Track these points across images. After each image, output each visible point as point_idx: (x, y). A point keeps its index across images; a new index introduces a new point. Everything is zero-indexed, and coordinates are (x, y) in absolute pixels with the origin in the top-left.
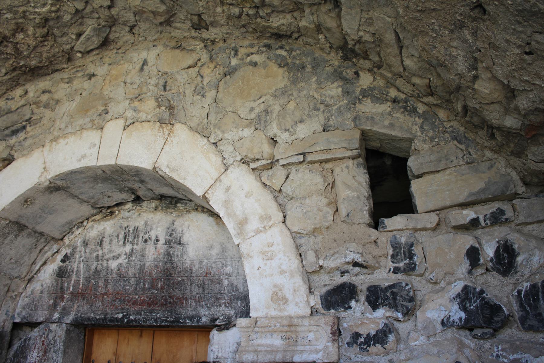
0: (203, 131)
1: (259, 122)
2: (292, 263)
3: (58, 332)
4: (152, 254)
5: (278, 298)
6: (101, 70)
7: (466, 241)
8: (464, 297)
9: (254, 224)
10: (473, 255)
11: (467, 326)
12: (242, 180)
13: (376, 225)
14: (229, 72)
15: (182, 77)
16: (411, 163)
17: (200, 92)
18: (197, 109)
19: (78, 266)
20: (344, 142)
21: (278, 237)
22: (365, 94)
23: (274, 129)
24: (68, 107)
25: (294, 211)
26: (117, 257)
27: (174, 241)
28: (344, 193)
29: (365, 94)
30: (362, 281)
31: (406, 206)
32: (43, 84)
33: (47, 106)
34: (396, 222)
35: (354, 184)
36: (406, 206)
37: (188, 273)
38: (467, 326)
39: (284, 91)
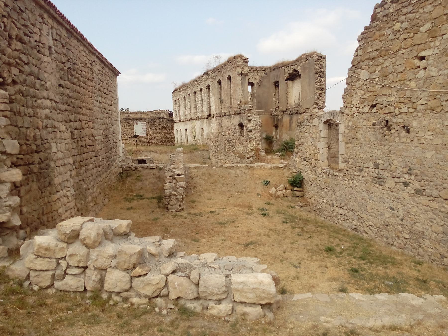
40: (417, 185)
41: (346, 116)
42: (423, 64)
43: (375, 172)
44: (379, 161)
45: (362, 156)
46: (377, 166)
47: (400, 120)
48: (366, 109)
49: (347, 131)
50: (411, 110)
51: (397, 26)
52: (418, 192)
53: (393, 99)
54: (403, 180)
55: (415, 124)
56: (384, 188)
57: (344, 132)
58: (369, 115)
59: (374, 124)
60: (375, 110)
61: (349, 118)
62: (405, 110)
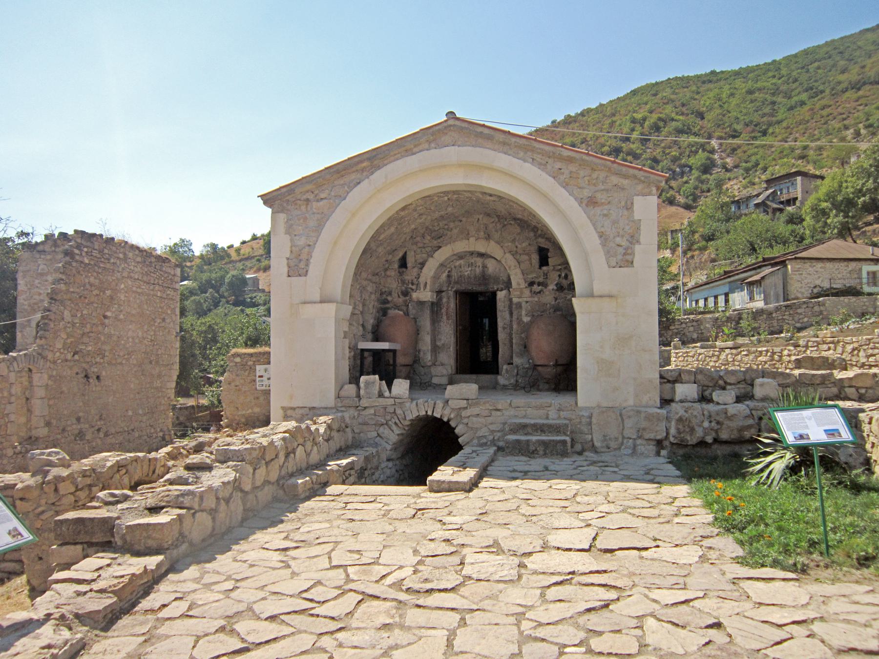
0: (498, 243)
1: (514, 241)
2: (521, 276)
3: (451, 293)
4: (478, 271)
5: (519, 284)
6: (464, 219)
7: (559, 273)
8: (556, 285)
9: (513, 268)
10: (560, 276)
11: (557, 290)
12: (508, 256)
13: (540, 268)
14: (504, 226)
15: (491, 226)
16: (549, 254)
17: (497, 231)
18: (496, 236)
19: (454, 274)
20: (534, 248)
21: (518, 271)
22: (540, 236)
23: (517, 243)
24: (455, 231)
25: (522, 265)
26: (467, 271)
27: (485, 267)
28: (534, 261)
29: (540, 236)
30: (537, 281)
31: (547, 264)
32: (444, 222)
33: (448, 230)
34: (544, 268)
35: (535, 258)
36: (547, 264)
37: (490, 276)
38: (557, 290)
39: (519, 234)
40: (104, 429)
41: (48, 363)
42: (106, 321)
43: (76, 428)
44: (81, 414)
45: (66, 412)
46: (78, 419)
47: (96, 370)
48: (69, 356)
49: (50, 383)
50: (102, 361)
51: (92, 279)
52: (106, 435)
53: (90, 348)
54: (96, 428)
55: (104, 373)
56: (85, 441)
57: (47, 385)
58: (72, 363)
59: (77, 374)
60: (76, 357)
61: (52, 366)
62: (98, 360)
